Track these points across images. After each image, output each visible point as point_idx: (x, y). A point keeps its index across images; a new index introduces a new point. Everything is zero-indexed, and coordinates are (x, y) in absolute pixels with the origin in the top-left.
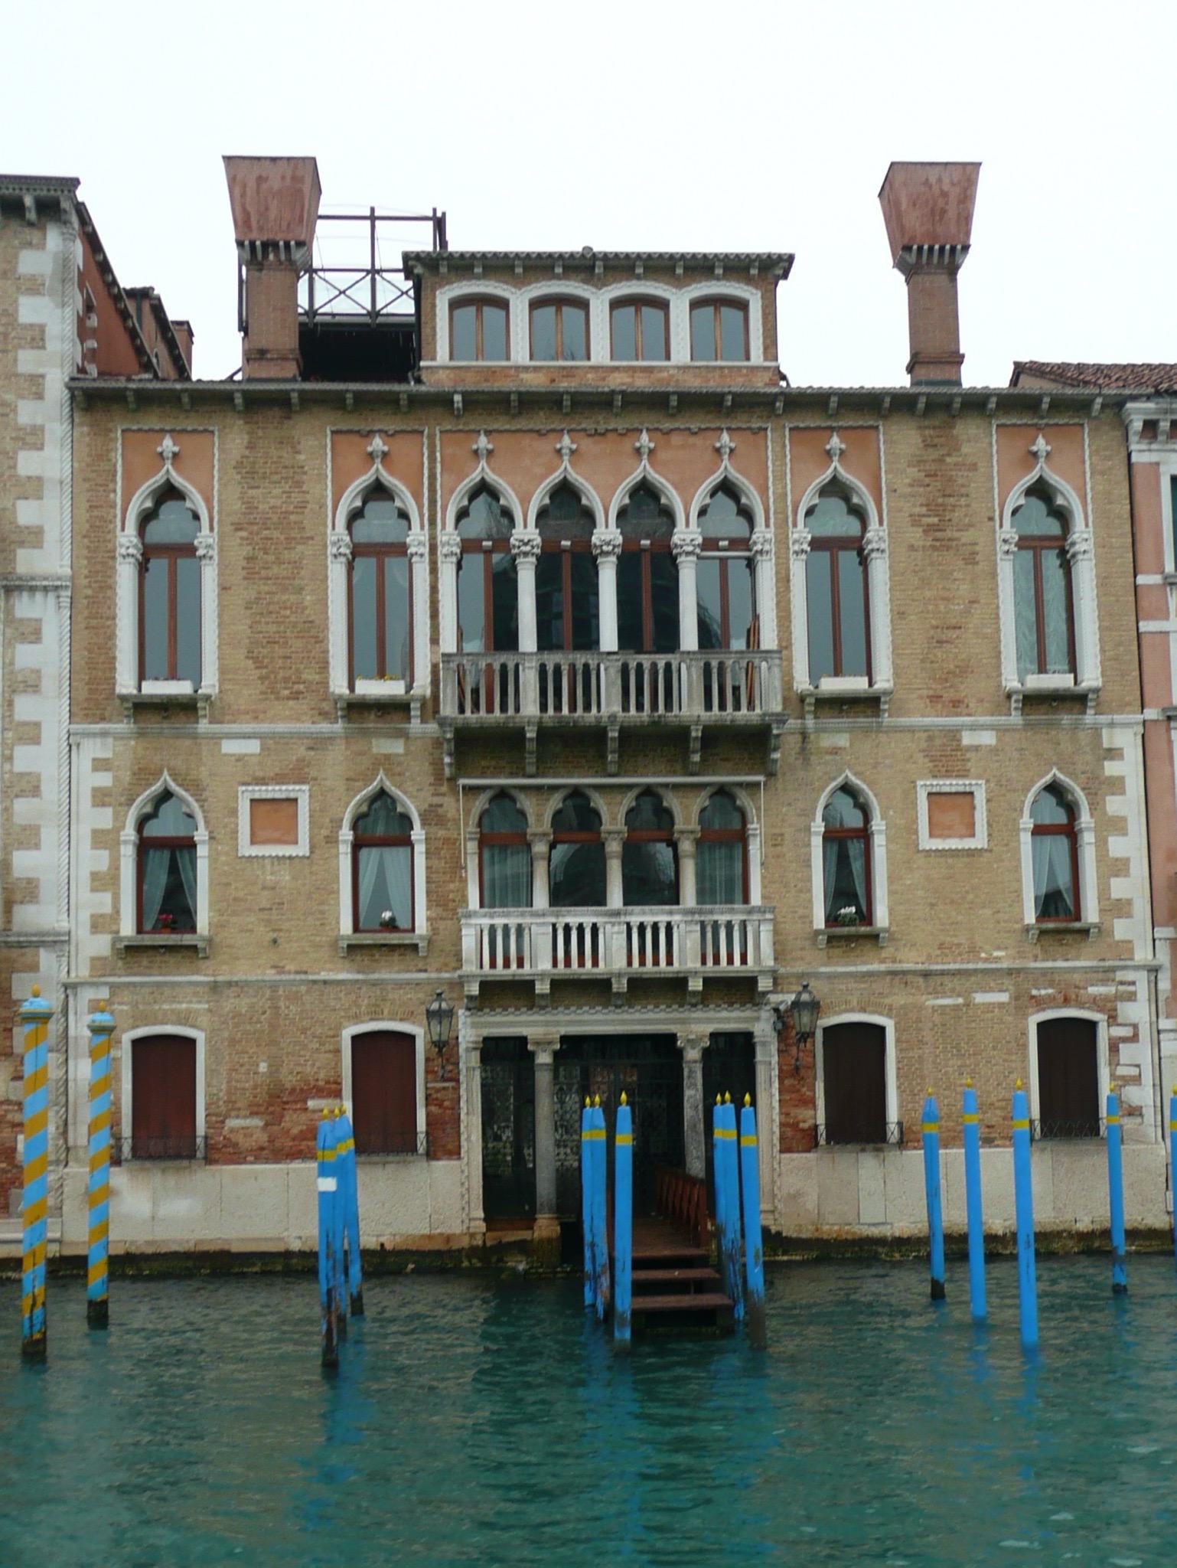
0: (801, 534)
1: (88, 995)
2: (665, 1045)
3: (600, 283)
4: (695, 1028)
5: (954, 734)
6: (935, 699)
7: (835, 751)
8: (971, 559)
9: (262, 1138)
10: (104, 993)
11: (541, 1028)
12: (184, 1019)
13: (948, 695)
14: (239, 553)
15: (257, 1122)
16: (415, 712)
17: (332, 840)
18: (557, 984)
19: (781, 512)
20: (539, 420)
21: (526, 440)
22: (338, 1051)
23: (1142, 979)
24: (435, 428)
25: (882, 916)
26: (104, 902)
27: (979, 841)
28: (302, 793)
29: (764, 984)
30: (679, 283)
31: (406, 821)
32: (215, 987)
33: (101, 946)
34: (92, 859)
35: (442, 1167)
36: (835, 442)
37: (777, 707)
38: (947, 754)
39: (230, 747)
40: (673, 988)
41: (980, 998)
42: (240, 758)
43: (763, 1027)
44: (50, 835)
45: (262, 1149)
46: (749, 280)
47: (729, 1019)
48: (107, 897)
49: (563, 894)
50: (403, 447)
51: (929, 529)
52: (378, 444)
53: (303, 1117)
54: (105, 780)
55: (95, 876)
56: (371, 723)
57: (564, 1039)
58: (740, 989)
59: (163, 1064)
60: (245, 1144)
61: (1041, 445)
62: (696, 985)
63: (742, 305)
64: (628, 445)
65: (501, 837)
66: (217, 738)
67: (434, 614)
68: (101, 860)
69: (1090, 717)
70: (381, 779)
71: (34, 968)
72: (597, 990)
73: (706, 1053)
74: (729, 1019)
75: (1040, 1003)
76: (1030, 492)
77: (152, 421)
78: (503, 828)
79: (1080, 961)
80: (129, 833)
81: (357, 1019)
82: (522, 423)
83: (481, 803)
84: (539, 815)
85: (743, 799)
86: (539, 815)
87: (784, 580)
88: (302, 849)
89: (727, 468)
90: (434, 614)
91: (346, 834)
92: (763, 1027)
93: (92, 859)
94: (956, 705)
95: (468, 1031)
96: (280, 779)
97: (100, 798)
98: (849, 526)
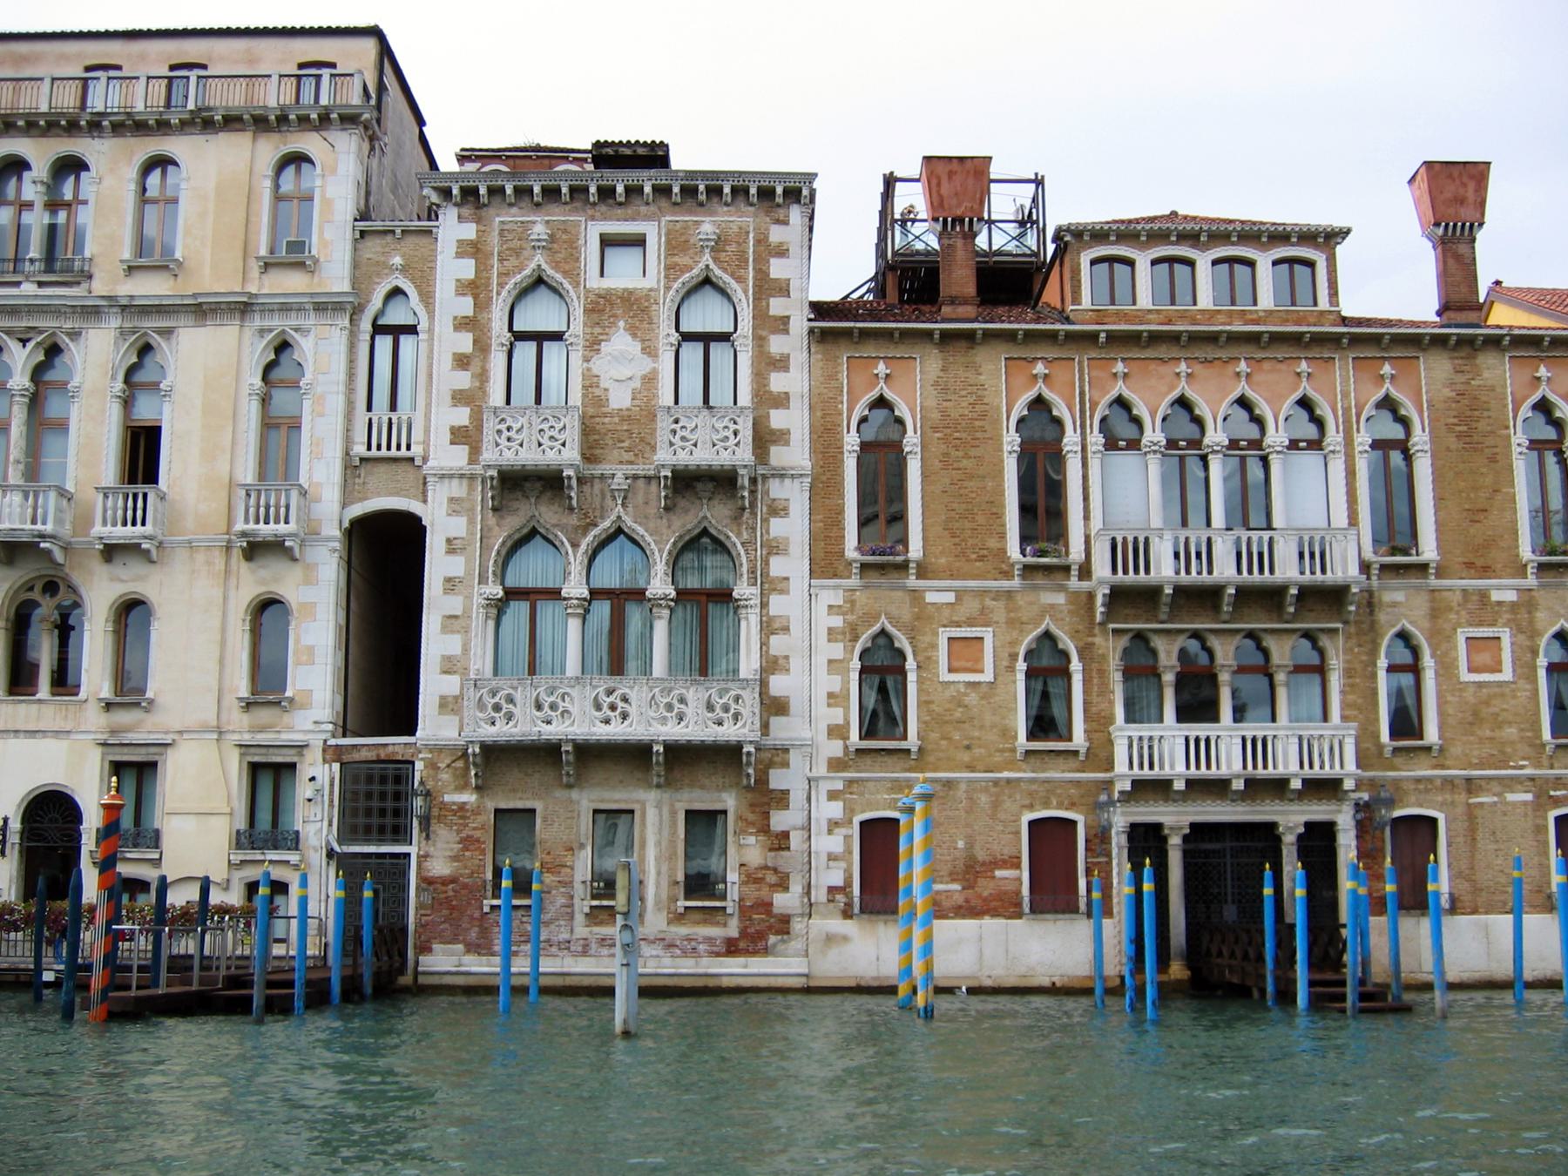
0: (1363, 439)
1: (825, 787)
2: (1268, 831)
3: (1204, 248)
4: (1291, 819)
6: (1469, 565)
7: (1394, 605)
8: (1493, 460)
9: (959, 899)
10: (839, 785)
11: (1175, 818)
13: (1480, 562)
14: (937, 449)
15: (956, 887)
16: (1074, 572)
17: (1011, 669)
18: (1190, 783)
19: (1347, 421)
20: (1162, 351)
21: (1152, 366)
22: (1018, 833)
25: (1432, 734)
26: (836, 715)
28: (988, 634)
29: (1348, 784)
30: (1264, 247)
31: (1065, 655)
34: (829, 682)
36: (1387, 369)
37: (1353, 571)
38: (1482, 609)
40: (1278, 786)
41: (1510, 797)
44: (796, 664)
45: (960, 907)
46: (1317, 246)
47: (1317, 811)
48: (839, 712)
49: (1186, 714)
50: (1059, 372)
52: (1040, 368)
53: (992, 884)
54: (837, 622)
55: (831, 695)
56: (1040, 580)
57: (1193, 826)
58: (1325, 788)
61: (1543, 372)
62: (1296, 784)
63: (1310, 264)
64: (1230, 369)
65: (1140, 670)
67: (1086, 498)
68: (835, 684)
71: (786, 764)
72: (1217, 788)
73: (1300, 837)
74: (1317, 811)
76: (1535, 407)
77: (869, 350)
78: (1046, 661)
80: (856, 664)
81: (1031, 807)
83: (1124, 641)
84: (1168, 654)
85: (1324, 641)
86: (1168, 654)
87: (1351, 473)
88: (987, 676)
89: (1305, 388)
90: (1086, 498)
91: (1021, 666)
92: (1345, 820)
93: (829, 682)
94: (1486, 571)
95: (1120, 820)
96: (971, 622)
98: (1397, 432)
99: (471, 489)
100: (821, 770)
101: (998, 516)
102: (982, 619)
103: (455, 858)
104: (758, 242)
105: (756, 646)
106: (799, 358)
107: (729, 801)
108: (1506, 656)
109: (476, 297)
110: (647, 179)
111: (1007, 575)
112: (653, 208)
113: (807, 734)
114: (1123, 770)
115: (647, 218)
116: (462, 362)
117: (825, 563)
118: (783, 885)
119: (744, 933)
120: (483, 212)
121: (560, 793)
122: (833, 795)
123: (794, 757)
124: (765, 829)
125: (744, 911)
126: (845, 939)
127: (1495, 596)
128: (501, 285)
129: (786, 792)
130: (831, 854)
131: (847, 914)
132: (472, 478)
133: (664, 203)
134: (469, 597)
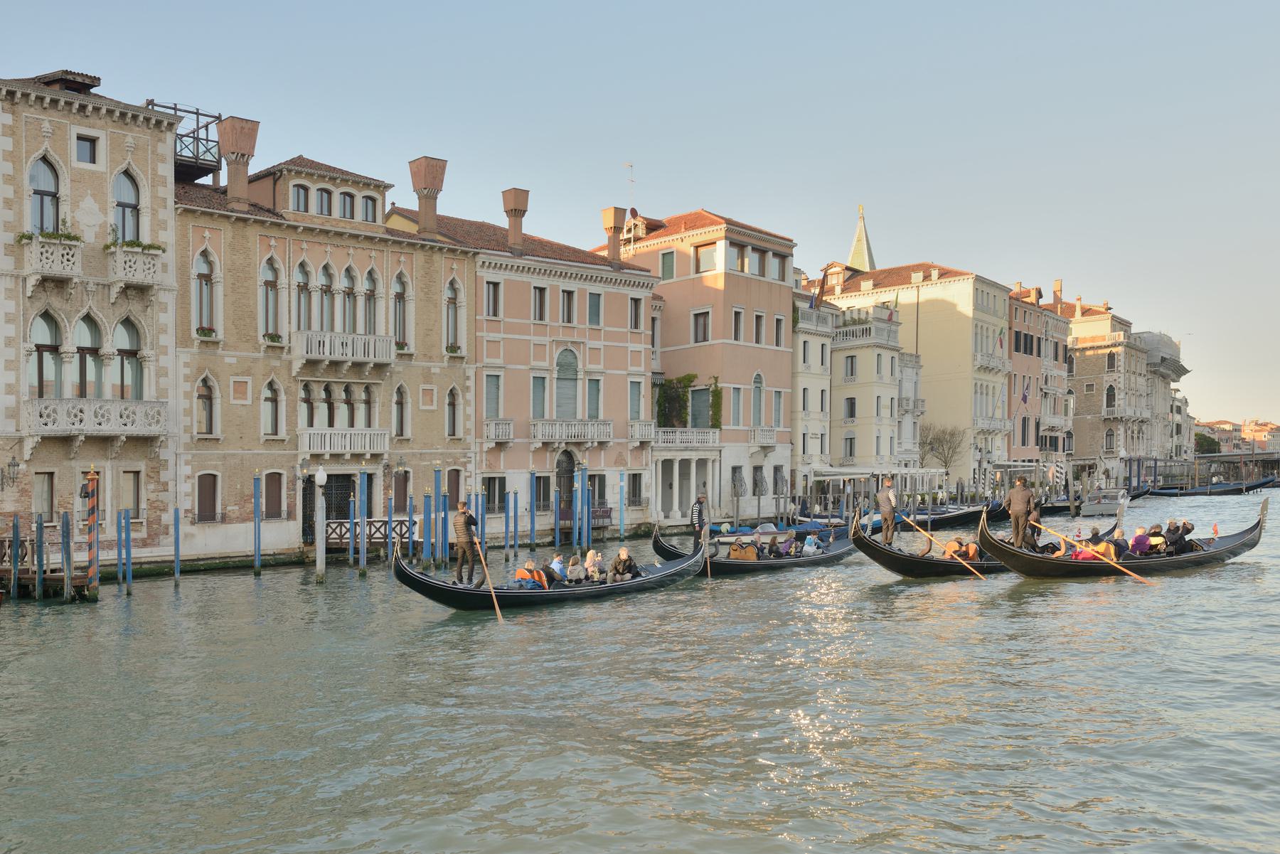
1: (184, 458)
5: (429, 368)
9: (237, 514)
12: (215, 467)
20: (322, 239)
21: (317, 246)
23: (472, 455)
24: (291, 236)
27: (434, 407)
28: (249, 379)
32: (225, 457)
33: (186, 438)
34: (184, 404)
35: (291, 523)
38: (428, 376)
39: (227, 360)
42: (230, 365)
43: (378, 471)
51: (426, 293)
54: (187, 371)
59: (208, 485)
60: (233, 516)
64: (346, 251)
66: (223, 357)
69: (464, 365)
70: (273, 376)
75: (449, 464)
79: (457, 451)
81: (266, 468)
82: (316, 239)
87: (387, 308)
88: (249, 402)
92: (378, 471)
96: (243, 374)
97: (187, 378)
99: (17, 283)
100: (181, 450)
101: (255, 319)
102: (247, 372)
103: (17, 501)
104: (153, 152)
105: (153, 383)
106: (171, 223)
107: (142, 466)
108: (435, 398)
109: (14, 163)
110: (78, 99)
111: (257, 349)
112: (102, 122)
113: (176, 431)
114: (304, 451)
115: (102, 128)
116: (8, 203)
117: (183, 341)
118: (165, 510)
119: (149, 535)
120: (16, 108)
121: (66, 463)
122: (187, 463)
123: (170, 442)
124: (158, 482)
125: (149, 523)
126: (193, 535)
127: (433, 370)
128: (27, 158)
129: (166, 461)
130: (186, 496)
131: (193, 523)
132: (17, 277)
133: (108, 120)
134: (18, 349)
